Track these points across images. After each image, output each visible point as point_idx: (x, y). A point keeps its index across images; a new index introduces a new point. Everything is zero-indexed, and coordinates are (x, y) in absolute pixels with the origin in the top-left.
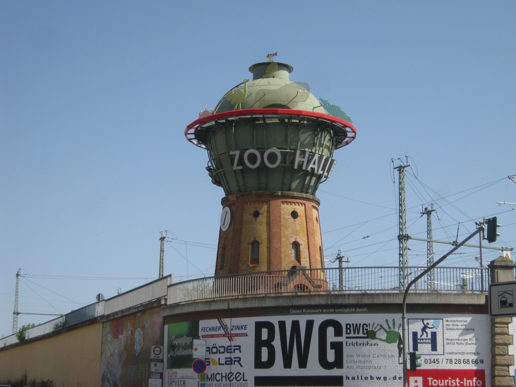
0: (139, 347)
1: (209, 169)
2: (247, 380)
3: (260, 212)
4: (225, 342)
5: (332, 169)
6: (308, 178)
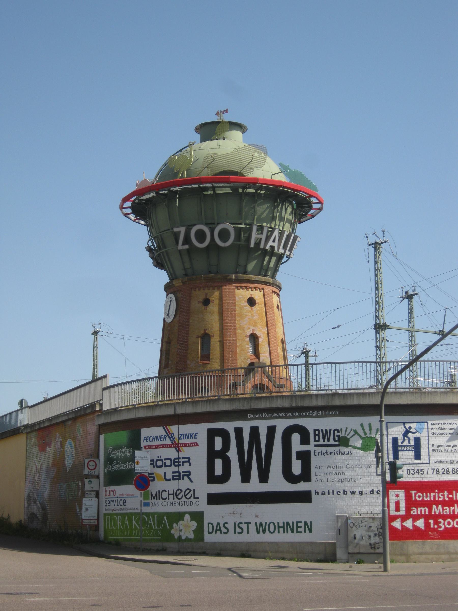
0: (70, 461)
1: (149, 249)
2: (198, 498)
3: (210, 299)
4: (171, 453)
5: (295, 247)
6: (267, 258)
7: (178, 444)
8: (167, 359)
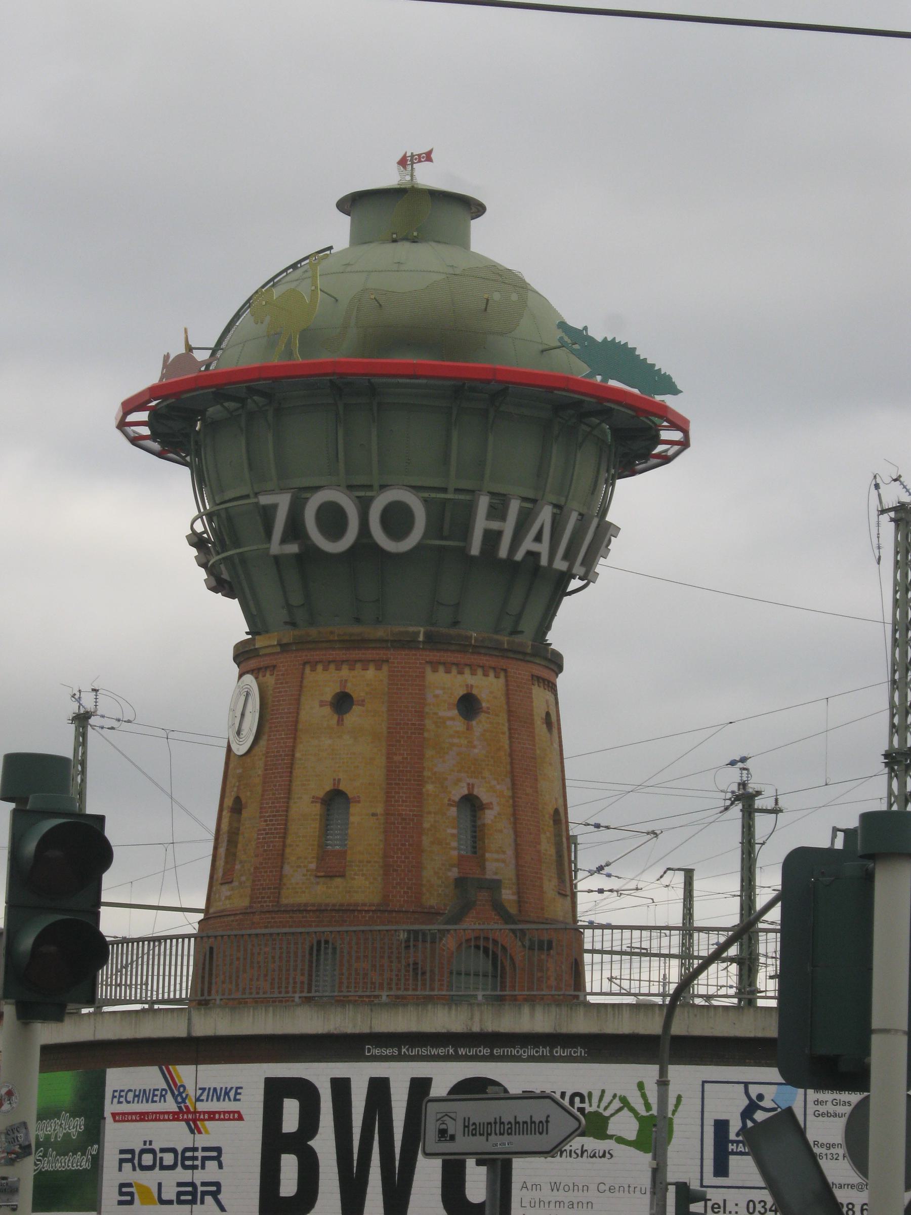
1: (197, 541)
4: (176, 1135)
7: (195, 1112)
8: (231, 855)
